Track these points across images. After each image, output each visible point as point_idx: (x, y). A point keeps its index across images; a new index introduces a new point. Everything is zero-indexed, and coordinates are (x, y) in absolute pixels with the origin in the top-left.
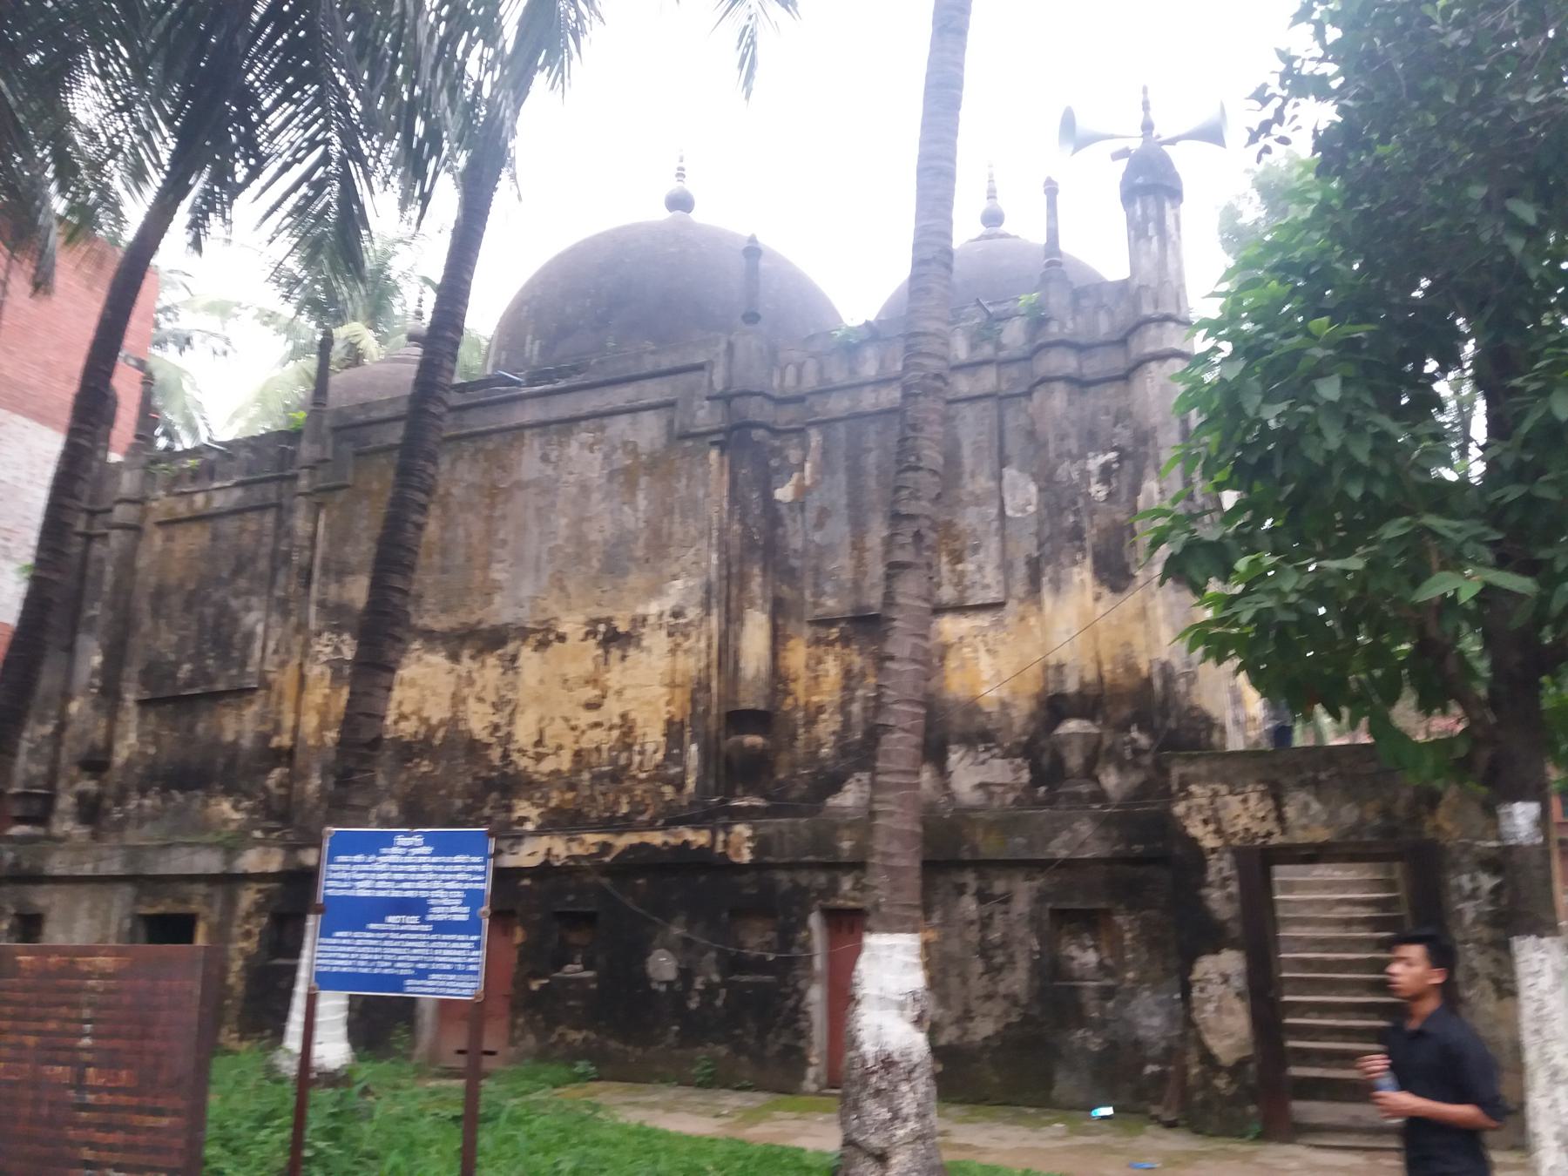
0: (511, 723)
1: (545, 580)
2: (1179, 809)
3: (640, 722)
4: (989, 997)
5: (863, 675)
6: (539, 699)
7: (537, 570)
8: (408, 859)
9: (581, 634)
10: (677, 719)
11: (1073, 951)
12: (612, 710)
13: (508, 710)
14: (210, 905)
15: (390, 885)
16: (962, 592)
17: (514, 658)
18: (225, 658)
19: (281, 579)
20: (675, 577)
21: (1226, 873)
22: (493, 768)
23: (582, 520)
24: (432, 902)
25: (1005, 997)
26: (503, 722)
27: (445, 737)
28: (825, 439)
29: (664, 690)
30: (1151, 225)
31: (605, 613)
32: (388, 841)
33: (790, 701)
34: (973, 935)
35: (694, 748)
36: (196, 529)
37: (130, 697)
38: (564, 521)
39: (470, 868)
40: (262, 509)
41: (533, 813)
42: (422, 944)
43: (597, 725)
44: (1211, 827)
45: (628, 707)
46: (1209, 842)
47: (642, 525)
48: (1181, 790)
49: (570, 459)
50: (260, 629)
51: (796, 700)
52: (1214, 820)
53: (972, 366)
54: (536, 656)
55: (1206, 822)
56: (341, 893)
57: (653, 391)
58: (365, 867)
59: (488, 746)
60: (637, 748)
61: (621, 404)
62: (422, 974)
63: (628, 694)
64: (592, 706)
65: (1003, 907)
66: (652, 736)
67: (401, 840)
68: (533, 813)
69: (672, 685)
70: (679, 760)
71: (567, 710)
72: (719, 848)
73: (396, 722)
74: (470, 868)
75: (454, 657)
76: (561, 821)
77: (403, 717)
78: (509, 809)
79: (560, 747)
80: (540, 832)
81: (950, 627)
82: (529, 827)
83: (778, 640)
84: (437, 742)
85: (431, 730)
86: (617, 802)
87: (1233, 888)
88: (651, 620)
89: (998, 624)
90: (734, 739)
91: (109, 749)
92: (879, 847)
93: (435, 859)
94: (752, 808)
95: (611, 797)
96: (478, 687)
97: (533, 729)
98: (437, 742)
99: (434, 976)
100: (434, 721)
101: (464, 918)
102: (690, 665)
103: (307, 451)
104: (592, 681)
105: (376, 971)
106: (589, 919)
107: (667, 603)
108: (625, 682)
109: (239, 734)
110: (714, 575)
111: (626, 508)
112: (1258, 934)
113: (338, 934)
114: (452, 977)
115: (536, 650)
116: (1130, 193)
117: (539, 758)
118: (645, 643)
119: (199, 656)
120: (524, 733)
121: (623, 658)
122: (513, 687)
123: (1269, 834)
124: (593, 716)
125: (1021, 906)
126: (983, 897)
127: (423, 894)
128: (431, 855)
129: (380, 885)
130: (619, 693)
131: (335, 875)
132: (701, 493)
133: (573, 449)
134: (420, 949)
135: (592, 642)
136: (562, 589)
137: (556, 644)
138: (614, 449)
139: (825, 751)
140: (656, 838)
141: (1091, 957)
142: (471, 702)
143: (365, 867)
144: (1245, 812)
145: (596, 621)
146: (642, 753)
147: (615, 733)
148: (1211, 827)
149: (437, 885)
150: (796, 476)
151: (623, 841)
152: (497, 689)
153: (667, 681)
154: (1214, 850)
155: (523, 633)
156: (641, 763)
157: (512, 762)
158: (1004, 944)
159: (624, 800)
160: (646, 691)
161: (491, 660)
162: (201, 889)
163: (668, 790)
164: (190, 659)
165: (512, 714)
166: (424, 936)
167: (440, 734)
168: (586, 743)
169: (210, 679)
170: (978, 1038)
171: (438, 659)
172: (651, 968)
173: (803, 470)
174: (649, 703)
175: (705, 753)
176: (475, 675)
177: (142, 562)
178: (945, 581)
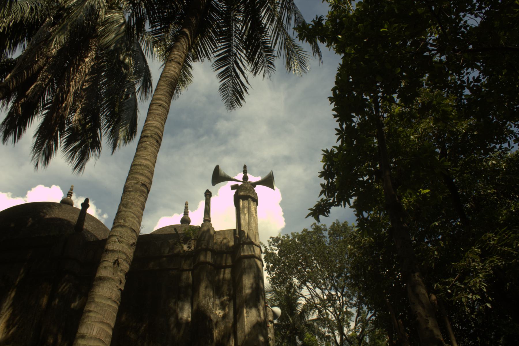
30: (246, 209)
116: (237, 199)
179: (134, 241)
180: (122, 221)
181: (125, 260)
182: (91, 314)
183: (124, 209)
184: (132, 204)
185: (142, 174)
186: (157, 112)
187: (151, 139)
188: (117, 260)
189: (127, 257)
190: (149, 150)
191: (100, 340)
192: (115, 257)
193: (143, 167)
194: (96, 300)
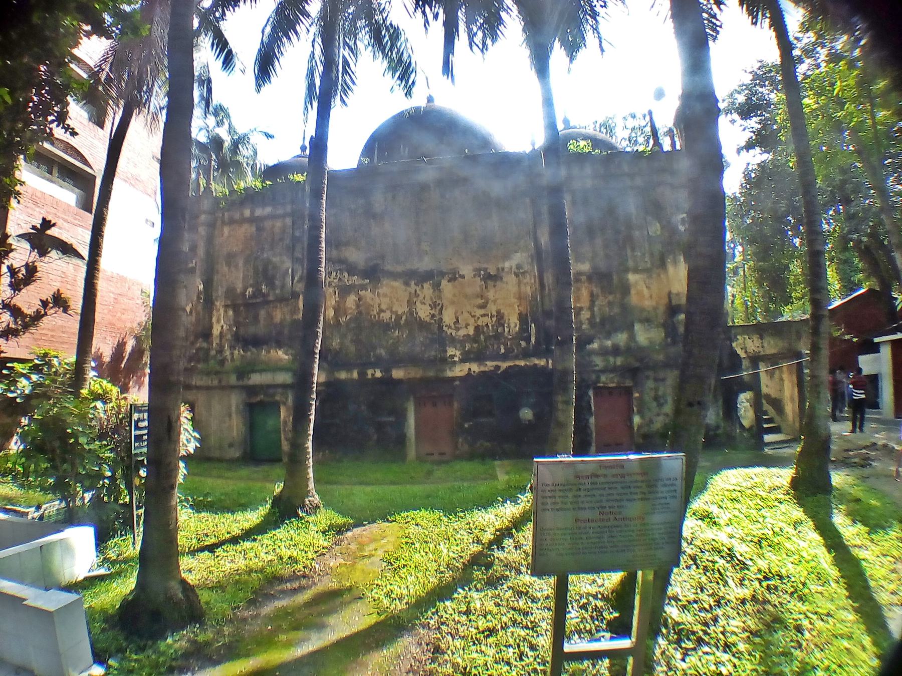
0: (441, 313)
4: (658, 415)
5: (598, 296)
6: (453, 303)
10: (524, 313)
12: (492, 308)
13: (438, 308)
14: (287, 399)
17: (439, 284)
20: (516, 252)
27: (406, 320)
31: (485, 266)
34: (652, 394)
36: (246, 226)
37: (218, 303)
40: (284, 216)
41: (458, 353)
43: (484, 315)
50: (290, 271)
52: (744, 349)
54: (450, 284)
59: (430, 324)
64: (483, 306)
66: (513, 323)
71: (469, 308)
72: (550, 366)
73: (378, 314)
75: (407, 284)
77: (381, 311)
80: (463, 361)
82: (456, 359)
84: (402, 322)
85: (398, 318)
88: (506, 270)
89: (650, 277)
95: (495, 346)
98: (402, 322)
100: (400, 313)
117: (457, 329)
118: (504, 279)
120: (448, 317)
121: (494, 286)
122: (440, 298)
124: (482, 312)
126: (656, 380)
130: (495, 301)
139: (584, 326)
145: (480, 270)
146: (509, 327)
147: (494, 319)
151: (504, 365)
152: (431, 299)
155: (442, 274)
159: (502, 347)
161: (426, 285)
162: (280, 390)
163: (523, 344)
164: (251, 286)
167: (404, 318)
169: (264, 295)
171: (397, 284)
177: (218, 241)
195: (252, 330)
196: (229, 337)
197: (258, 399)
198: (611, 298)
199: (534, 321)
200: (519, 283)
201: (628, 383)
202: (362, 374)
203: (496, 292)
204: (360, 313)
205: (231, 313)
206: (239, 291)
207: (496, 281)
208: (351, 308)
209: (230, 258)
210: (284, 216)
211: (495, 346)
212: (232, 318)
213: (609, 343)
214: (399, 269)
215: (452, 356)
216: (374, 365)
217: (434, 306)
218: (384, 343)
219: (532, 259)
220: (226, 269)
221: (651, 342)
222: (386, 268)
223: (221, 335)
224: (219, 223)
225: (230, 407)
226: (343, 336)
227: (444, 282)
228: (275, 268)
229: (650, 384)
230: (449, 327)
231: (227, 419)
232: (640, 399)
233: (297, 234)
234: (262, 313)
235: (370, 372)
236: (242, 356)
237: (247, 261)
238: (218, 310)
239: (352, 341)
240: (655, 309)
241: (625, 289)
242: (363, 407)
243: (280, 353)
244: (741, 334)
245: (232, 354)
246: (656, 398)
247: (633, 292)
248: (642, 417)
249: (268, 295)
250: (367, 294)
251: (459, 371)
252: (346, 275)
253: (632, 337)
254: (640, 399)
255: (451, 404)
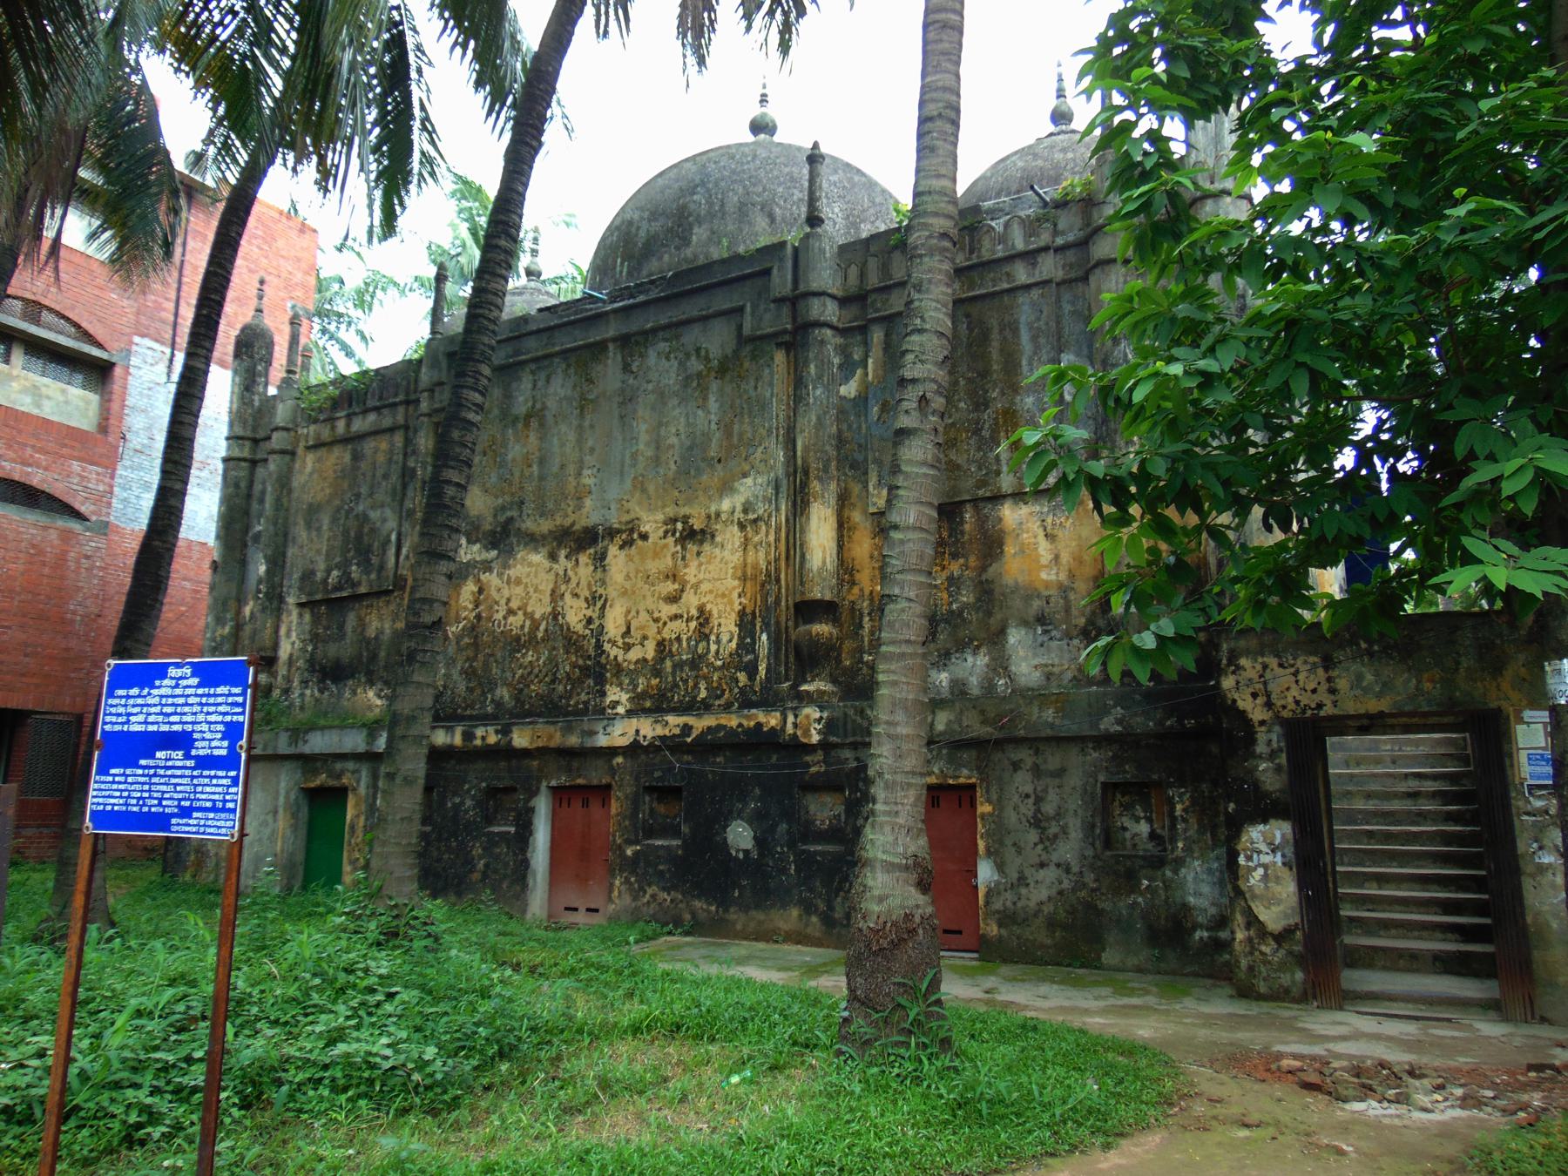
0: (602, 616)
1: (628, 484)
2: (1228, 683)
3: (715, 612)
4: (1042, 865)
6: (624, 593)
7: (622, 474)
8: (178, 691)
9: (661, 533)
10: (748, 611)
11: (1126, 821)
12: (691, 601)
14: (358, 782)
15: (160, 719)
16: (1020, 479)
18: (366, 564)
19: (410, 493)
20: (745, 475)
21: (1275, 745)
22: (589, 657)
23: (660, 424)
24: (196, 736)
25: (1058, 865)
26: (595, 616)
28: (886, 335)
29: (736, 583)
32: (161, 671)
33: (856, 590)
34: (1028, 808)
35: (764, 637)
36: (337, 451)
37: (291, 600)
38: (643, 427)
39: (230, 700)
40: (391, 430)
41: (624, 697)
42: (185, 781)
43: (676, 617)
44: (1260, 701)
45: (704, 600)
46: (1257, 713)
47: (714, 426)
48: (1229, 665)
49: (649, 368)
50: (393, 537)
51: (862, 590)
53: (1030, 256)
54: (623, 553)
55: (1254, 695)
56: (117, 728)
57: (722, 301)
58: (140, 701)
59: (584, 637)
60: (713, 638)
61: (695, 313)
62: (186, 812)
63: (705, 587)
64: (673, 599)
65: (1057, 781)
66: (727, 627)
67: (172, 672)
68: (624, 697)
69: (744, 579)
70: (751, 649)
71: (650, 603)
72: (790, 729)
73: (505, 618)
74: (230, 700)
75: (553, 557)
76: (653, 704)
77: (511, 612)
78: (603, 694)
79: (645, 638)
80: (630, 713)
81: (1010, 514)
83: (843, 528)
84: (540, 635)
86: (696, 685)
87: (1283, 759)
90: (802, 628)
91: (276, 646)
92: (883, 717)
93: (200, 691)
94: (821, 693)
95: (691, 683)
96: (573, 584)
97: (621, 621)
98: (540, 635)
99: (195, 815)
100: (537, 616)
101: (224, 752)
102: (760, 558)
103: (425, 376)
104: (673, 576)
105: (146, 809)
106: (675, 792)
107: (739, 500)
108: (701, 576)
109: (380, 632)
110: (781, 472)
111: (700, 412)
112: (1307, 806)
113: (113, 771)
114: (212, 815)
115: (621, 547)
117: (627, 647)
118: (718, 539)
119: (344, 566)
120: (613, 624)
121: (699, 554)
122: (603, 583)
123: (1320, 706)
124: (673, 609)
125: (1075, 780)
126: (1037, 771)
127: (189, 728)
128: (197, 687)
129: (151, 719)
131: (113, 710)
132: (768, 395)
133: (652, 358)
134: (184, 785)
135: (670, 540)
136: (644, 490)
137: (640, 542)
138: (688, 355)
140: (733, 721)
141: (1144, 828)
142: (568, 596)
143: (140, 701)
144: (1296, 685)
145: (674, 521)
146: (718, 642)
147: (693, 624)
148: (1260, 701)
149: (201, 718)
150: (859, 372)
151: (700, 724)
152: (589, 585)
153: (739, 573)
154: (1262, 723)
155: (611, 533)
156: (717, 652)
157: (603, 652)
158: (1059, 815)
159: (703, 685)
160: (719, 582)
161: (583, 558)
162: (350, 765)
163: (742, 677)
164: (338, 567)
165: (603, 607)
166: (187, 772)
167: (542, 627)
168: (666, 634)
169: (354, 585)
170: (1032, 904)
171: (538, 558)
172: (730, 837)
173: (866, 367)
174: (723, 595)
175: (775, 641)
176: (570, 573)
177: (297, 481)
178: (1005, 469)
179: (946, 353)
180: (918, 321)
181: (938, 392)
182: (901, 492)
183: (917, 296)
184: (930, 281)
185: (936, 214)
186: (940, 46)
187: (939, 123)
188: (924, 396)
189: (940, 386)
190: (941, 152)
191: (922, 529)
192: (918, 391)
193: (936, 197)
194: (904, 468)
195: (333, 650)
196: (301, 663)
197: (318, 782)
198: (955, 568)
199: (766, 626)
200: (746, 543)
201: (965, 776)
202: (469, 736)
203: (700, 565)
204: (478, 617)
205: (307, 617)
206: (319, 576)
207: (701, 542)
208: (465, 608)
209: (313, 510)
210: (391, 430)
211: (691, 683)
212: (307, 628)
213: (943, 678)
214: (545, 526)
215: (616, 704)
216: (485, 719)
217: (592, 600)
218: (508, 675)
219: (777, 489)
220: (304, 534)
221: (1048, 676)
222: (523, 526)
223: (291, 661)
224: (302, 444)
225: (277, 792)
226: (451, 662)
227: (613, 550)
228: (373, 530)
229: (1023, 782)
230: (614, 643)
231: (270, 818)
232: (997, 820)
233: (411, 464)
234: (351, 620)
235: (479, 732)
236: (317, 700)
237: (334, 520)
238: (289, 613)
239: (463, 672)
240: (1064, 590)
241: (992, 545)
242: (469, 803)
243: (371, 694)
244: (1253, 654)
245: (302, 695)
246: (1037, 822)
247: (1010, 549)
248: (1000, 867)
249: (359, 583)
250: (491, 579)
251: (619, 734)
252: (463, 541)
253: (1000, 665)
254: (997, 820)
255: (605, 803)
